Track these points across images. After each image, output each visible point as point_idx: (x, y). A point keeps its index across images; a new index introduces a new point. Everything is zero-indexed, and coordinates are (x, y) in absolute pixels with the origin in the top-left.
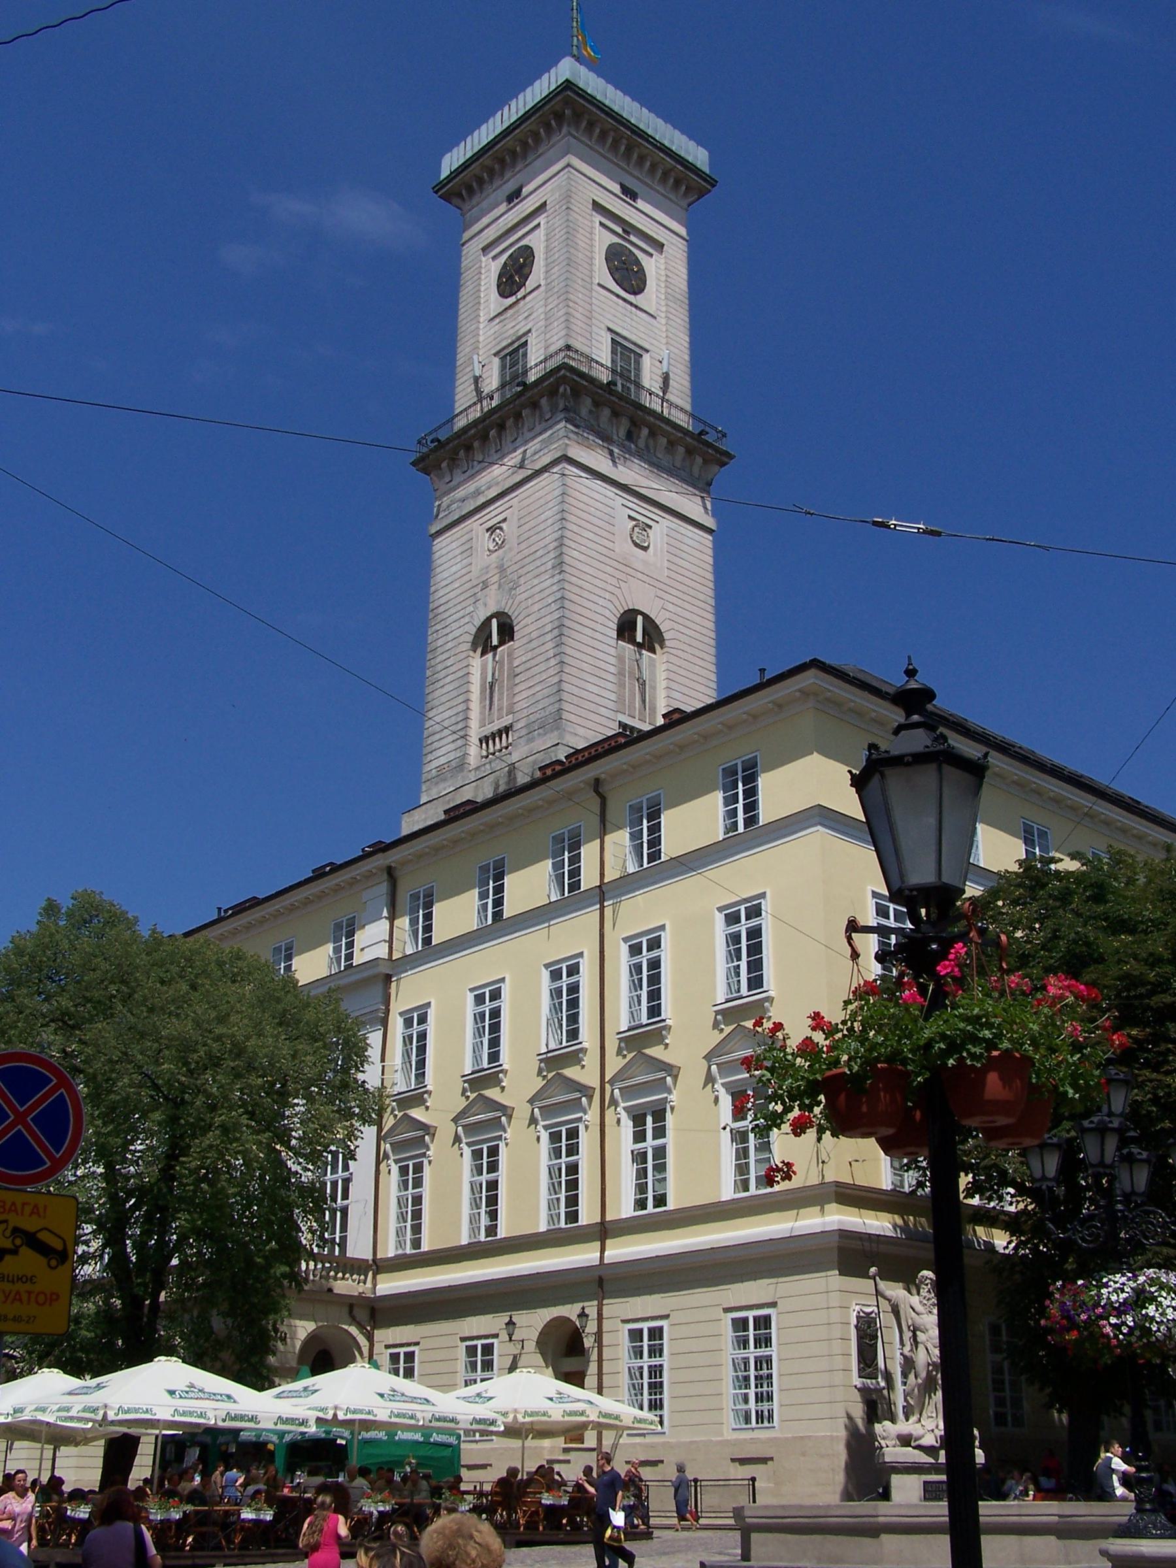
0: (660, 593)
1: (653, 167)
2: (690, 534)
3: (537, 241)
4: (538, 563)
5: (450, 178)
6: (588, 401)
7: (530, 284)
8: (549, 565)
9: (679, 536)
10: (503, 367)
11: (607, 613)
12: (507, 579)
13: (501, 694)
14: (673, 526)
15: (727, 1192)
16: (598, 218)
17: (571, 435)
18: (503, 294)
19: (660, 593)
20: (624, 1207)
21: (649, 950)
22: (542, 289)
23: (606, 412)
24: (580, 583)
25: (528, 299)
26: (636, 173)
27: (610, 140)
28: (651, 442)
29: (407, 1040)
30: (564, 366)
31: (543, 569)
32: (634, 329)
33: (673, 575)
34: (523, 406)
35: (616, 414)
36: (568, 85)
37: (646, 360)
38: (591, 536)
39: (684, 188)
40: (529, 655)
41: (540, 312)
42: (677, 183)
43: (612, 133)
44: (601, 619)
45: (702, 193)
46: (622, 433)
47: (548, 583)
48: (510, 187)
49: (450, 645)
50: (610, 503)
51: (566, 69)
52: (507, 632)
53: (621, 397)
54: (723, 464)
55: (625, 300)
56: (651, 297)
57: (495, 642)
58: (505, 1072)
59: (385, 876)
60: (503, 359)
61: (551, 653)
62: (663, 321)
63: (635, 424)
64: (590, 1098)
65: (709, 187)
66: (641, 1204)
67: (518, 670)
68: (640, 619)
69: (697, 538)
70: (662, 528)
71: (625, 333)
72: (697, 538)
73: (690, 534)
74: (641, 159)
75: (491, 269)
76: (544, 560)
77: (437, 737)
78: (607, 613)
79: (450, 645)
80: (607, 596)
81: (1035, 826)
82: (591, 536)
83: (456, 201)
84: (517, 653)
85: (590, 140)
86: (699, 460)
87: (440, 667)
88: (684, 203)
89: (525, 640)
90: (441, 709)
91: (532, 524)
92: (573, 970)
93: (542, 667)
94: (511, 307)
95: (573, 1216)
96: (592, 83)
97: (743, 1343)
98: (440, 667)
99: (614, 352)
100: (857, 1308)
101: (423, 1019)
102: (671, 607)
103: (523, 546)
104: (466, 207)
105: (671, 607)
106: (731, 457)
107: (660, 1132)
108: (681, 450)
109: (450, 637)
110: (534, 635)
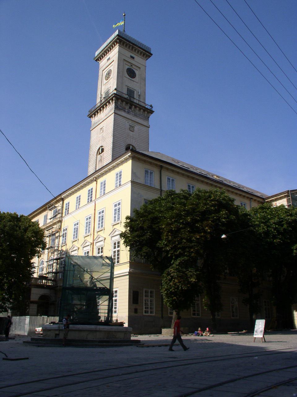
1: (138, 52)
3: (111, 68)
6: (120, 101)
7: (111, 77)
10: (105, 95)
11: (123, 145)
12: (104, 139)
16: (125, 62)
26: (134, 53)
28: (135, 109)
34: (107, 102)
35: (127, 103)
37: (135, 92)
39: (145, 56)
43: (128, 45)
45: (150, 57)
48: (108, 58)
52: (103, 150)
54: (152, 113)
55: (131, 80)
57: (101, 152)
65: (151, 55)
67: (104, 158)
70: (137, 128)
75: (105, 74)
81: (191, 185)
83: (98, 61)
84: (104, 154)
86: (146, 112)
88: (146, 59)
90: (91, 167)
92: (90, 218)
93: (108, 157)
94: (107, 82)
99: (128, 90)
104: (100, 62)
106: (153, 112)
108: (142, 110)
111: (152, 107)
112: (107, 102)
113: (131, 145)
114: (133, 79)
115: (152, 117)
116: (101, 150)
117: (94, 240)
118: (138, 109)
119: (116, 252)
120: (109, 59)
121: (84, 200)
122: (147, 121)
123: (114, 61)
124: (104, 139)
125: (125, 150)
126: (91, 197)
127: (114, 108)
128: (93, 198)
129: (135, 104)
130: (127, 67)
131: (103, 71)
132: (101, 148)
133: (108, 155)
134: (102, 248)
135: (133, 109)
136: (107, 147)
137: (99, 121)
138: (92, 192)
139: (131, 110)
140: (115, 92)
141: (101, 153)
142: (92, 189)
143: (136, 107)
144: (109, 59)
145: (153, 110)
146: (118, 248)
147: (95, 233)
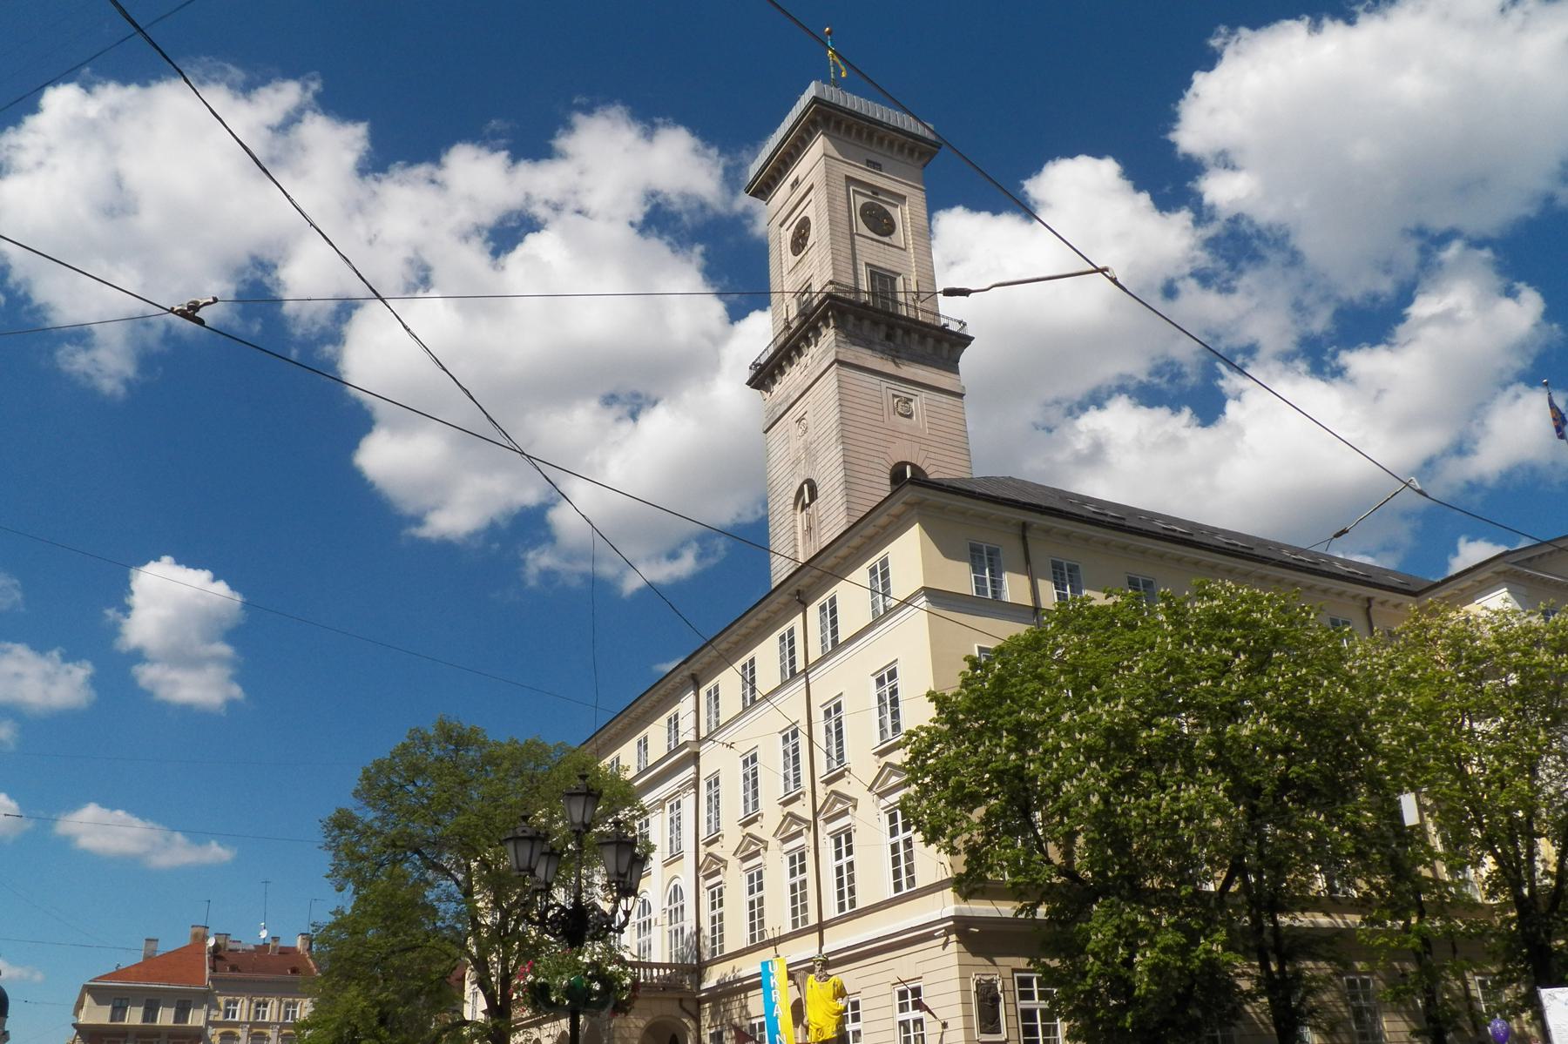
0: (923, 447)
2: (944, 400)
3: (810, 212)
4: (827, 440)
5: (754, 181)
7: (810, 243)
8: (834, 439)
9: (935, 403)
11: (881, 468)
12: (810, 452)
13: (815, 537)
14: (929, 396)
15: (890, 893)
17: (841, 344)
18: (795, 254)
19: (923, 447)
20: (831, 911)
21: (835, 713)
22: (816, 245)
23: (866, 323)
24: (857, 449)
25: (809, 253)
27: (854, 131)
28: (906, 339)
29: (709, 799)
30: (829, 295)
31: (830, 443)
32: (885, 258)
33: (931, 431)
34: (808, 331)
35: (875, 323)
36: (815, 100)
38: (862, 414)
39: (916, 154)
40: (827, 507)
41: (816, 262)
42: (912, 152)
43: (855, 127)
44: (877, 473)
45: (932, 155)
46: (882, 335)
47: (834, 453)
49: (781, 508)
50: (878, 388)
51: (812, 91)
52: (813, 495)
53: (876, 311)
54: (966, 345)
56: (898, 237)
58: (762, 815)
59: (692, 682)
60: (798, 299)
61: (840, 503)
62: (912, 251)
63: (891, 327)
64: (809, 830)
65: (936, 149)
66: (841, 907)
67: (822, 519)
68: (908, 468)
69: (951, 402)
70: (920, 401)
71: (881, 265)
72: (951, 402)
73: (944, 400)
74: (881, 140)
75: (787, 235)
76: (830, 437)
77: (779, 575)
78: (881, 468)
79: (781, 508)
80: (881, 455)
81: (1140, 578)
82: (862, 414)
85: (839, 133)
86: (946, 346)
87: (777, 524)
88: (920, 164)
89: (823, 497)
91: (822, 412)
92: (795, 734)
93: (836, 514)
95: (805, 919)
96: (833, 95)
97: (903, 1008)
98: (777, 524)
99: (872, 280)
100: (978, 978)
101: (717, 783)
102: (933, 455)
103: (818, 429)
105: (933, 455)
107: (850, 851)
108: (930, 341)
109: (781, 502)
110: (830, 491)
111: (965, 324)
112: (808, 331)
113: (906, 463)
114: (886, 239)
115: (967, 358)
116: (808, 492)
117: (816, 814)
118: (915, 337)
119: (901, 846)
120: (796, 183)
121: (768, 676)
122: (953, 376)
123: (811, 187)
124: (810, 452)
125: (888, 482)
126: (792, 662)
127: (834, 344)
128: (800, 666)
129: (903, 322)
130: (861, 200)
131: (781, 225)
132: (805, 486)
133: (834, 508)
134: (849, 838)
135: (898, 340)
136: (828, 479)
137: (788, 396)
138: (792, 642)
139: (892, 344)
140: (829, 288)
141: (809, 505)
142: (791, 632)
143: (907, 332)
144: (796, 183)
145: (970, 334)
146: (904, 831)
147: (820, 787)
